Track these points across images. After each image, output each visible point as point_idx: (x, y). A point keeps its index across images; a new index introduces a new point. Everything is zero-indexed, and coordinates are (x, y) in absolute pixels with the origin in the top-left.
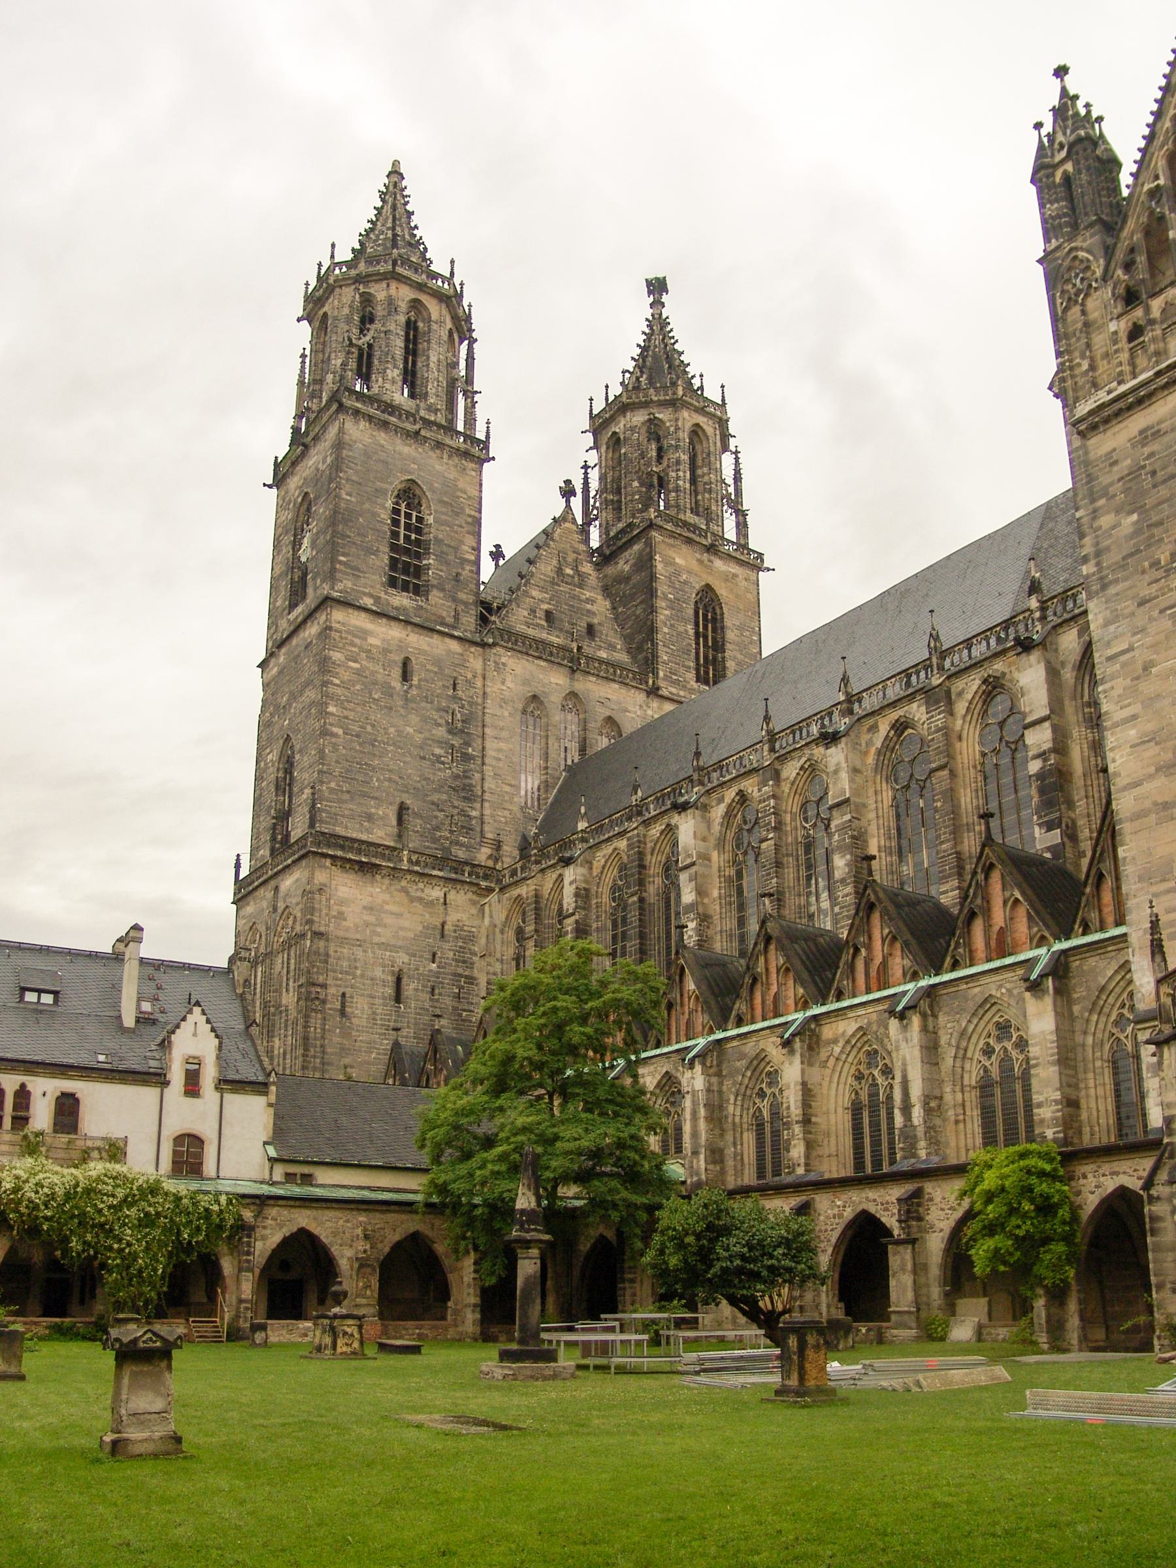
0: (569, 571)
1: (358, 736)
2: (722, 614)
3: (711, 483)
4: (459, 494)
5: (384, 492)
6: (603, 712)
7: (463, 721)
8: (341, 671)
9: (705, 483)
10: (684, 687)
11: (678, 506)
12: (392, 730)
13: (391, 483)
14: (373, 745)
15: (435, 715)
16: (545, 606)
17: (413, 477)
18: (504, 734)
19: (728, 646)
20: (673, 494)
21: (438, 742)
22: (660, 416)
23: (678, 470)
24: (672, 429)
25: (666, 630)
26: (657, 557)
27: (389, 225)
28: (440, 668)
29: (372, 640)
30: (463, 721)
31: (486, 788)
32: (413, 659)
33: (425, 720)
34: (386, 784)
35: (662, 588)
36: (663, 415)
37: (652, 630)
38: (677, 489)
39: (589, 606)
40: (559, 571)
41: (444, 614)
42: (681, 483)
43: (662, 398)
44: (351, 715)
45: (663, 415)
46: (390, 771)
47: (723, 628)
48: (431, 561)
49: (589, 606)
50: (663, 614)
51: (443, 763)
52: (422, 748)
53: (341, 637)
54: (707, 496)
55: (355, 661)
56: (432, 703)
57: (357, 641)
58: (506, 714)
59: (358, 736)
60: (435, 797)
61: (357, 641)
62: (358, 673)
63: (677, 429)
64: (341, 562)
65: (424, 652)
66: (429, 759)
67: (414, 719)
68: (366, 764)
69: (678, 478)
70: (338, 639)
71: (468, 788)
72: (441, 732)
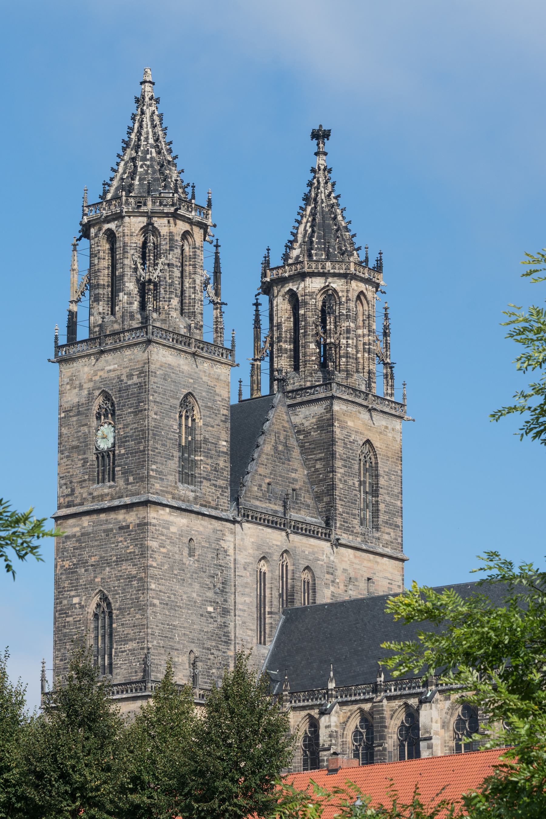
0: (281, 448)
1: (167, 604)
2: (377, 463)
3: (370, 344)
4: (217, 398)
5: (173, 407)
6: (304, 563)
7: (223, 583)
8: (156, 556)
9: (364, 344)
10: (352, 531)
11: (347, 371)
12: (185, 597)
13: (178, 399)
14: (175, 610)
15: (208, 581)
16: (267, 480)
17: (190, 391)
18: (247, 590)
19: (381, 491)
20: (344, 360)
21: (211, 602)
22: (334, 286)
23: (348, 338)
24: (344, 299)
25: (341, 486)
26: (336, 424)
27: (151, 141)
28: (209, 542)
29: (173, 529)
30: (223, 583)
31: (237, 635)
32: (194, 539)
33: (203, 585)
34: (183, 638)
35: (339, 449)
36: (337, 284)
37: (332, 487)
38: (347, 356)
39: (293, 475)
40: (275, 448)
41: (210, 499)
42: (350, 350)
43: (337, 271)
44: (163, 588)
45: (337, 284)
46: (184, 628)
47: (377, 476)
48: (202, 458)
49: (293, 475)
50: (340, 472)
51: (212, 617)
52: (201, 607)
53: (156, 530)
54: (366, 355)
55: (164, 547)
56: (205, 572)
57: (165, 531)
58: (248, 574)
59: (167, 604)
60: (208, 644)
61: (165, 531)
62: (166, 556)
63: (348, 300)
64: (152, 470)
65: (200, 533)
66: (205, 616)
67: (196, 586)
68: (172, 625)
69: (348, 345)
70: (154, 532)
71: (226, 635)
72: (210, 594)
